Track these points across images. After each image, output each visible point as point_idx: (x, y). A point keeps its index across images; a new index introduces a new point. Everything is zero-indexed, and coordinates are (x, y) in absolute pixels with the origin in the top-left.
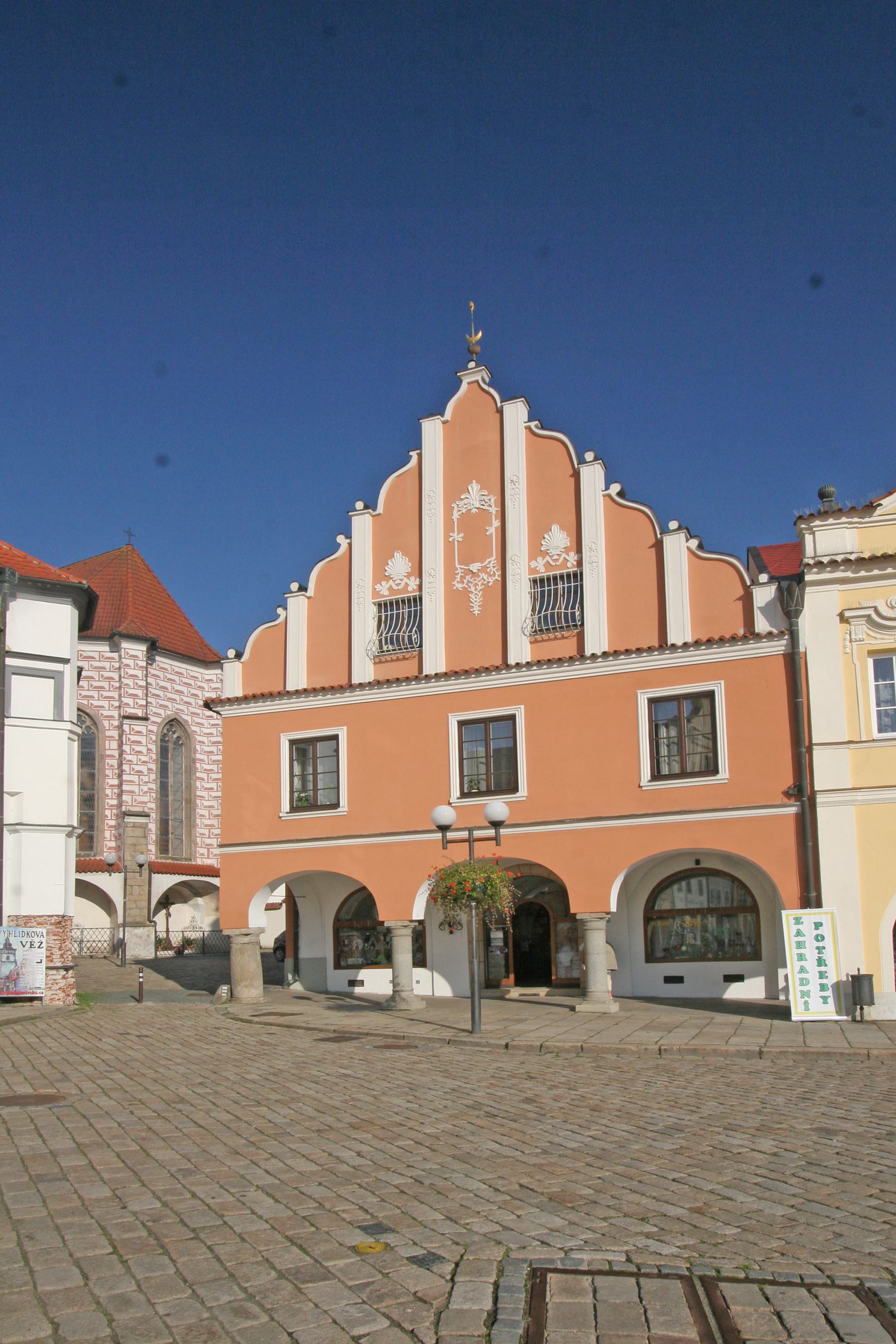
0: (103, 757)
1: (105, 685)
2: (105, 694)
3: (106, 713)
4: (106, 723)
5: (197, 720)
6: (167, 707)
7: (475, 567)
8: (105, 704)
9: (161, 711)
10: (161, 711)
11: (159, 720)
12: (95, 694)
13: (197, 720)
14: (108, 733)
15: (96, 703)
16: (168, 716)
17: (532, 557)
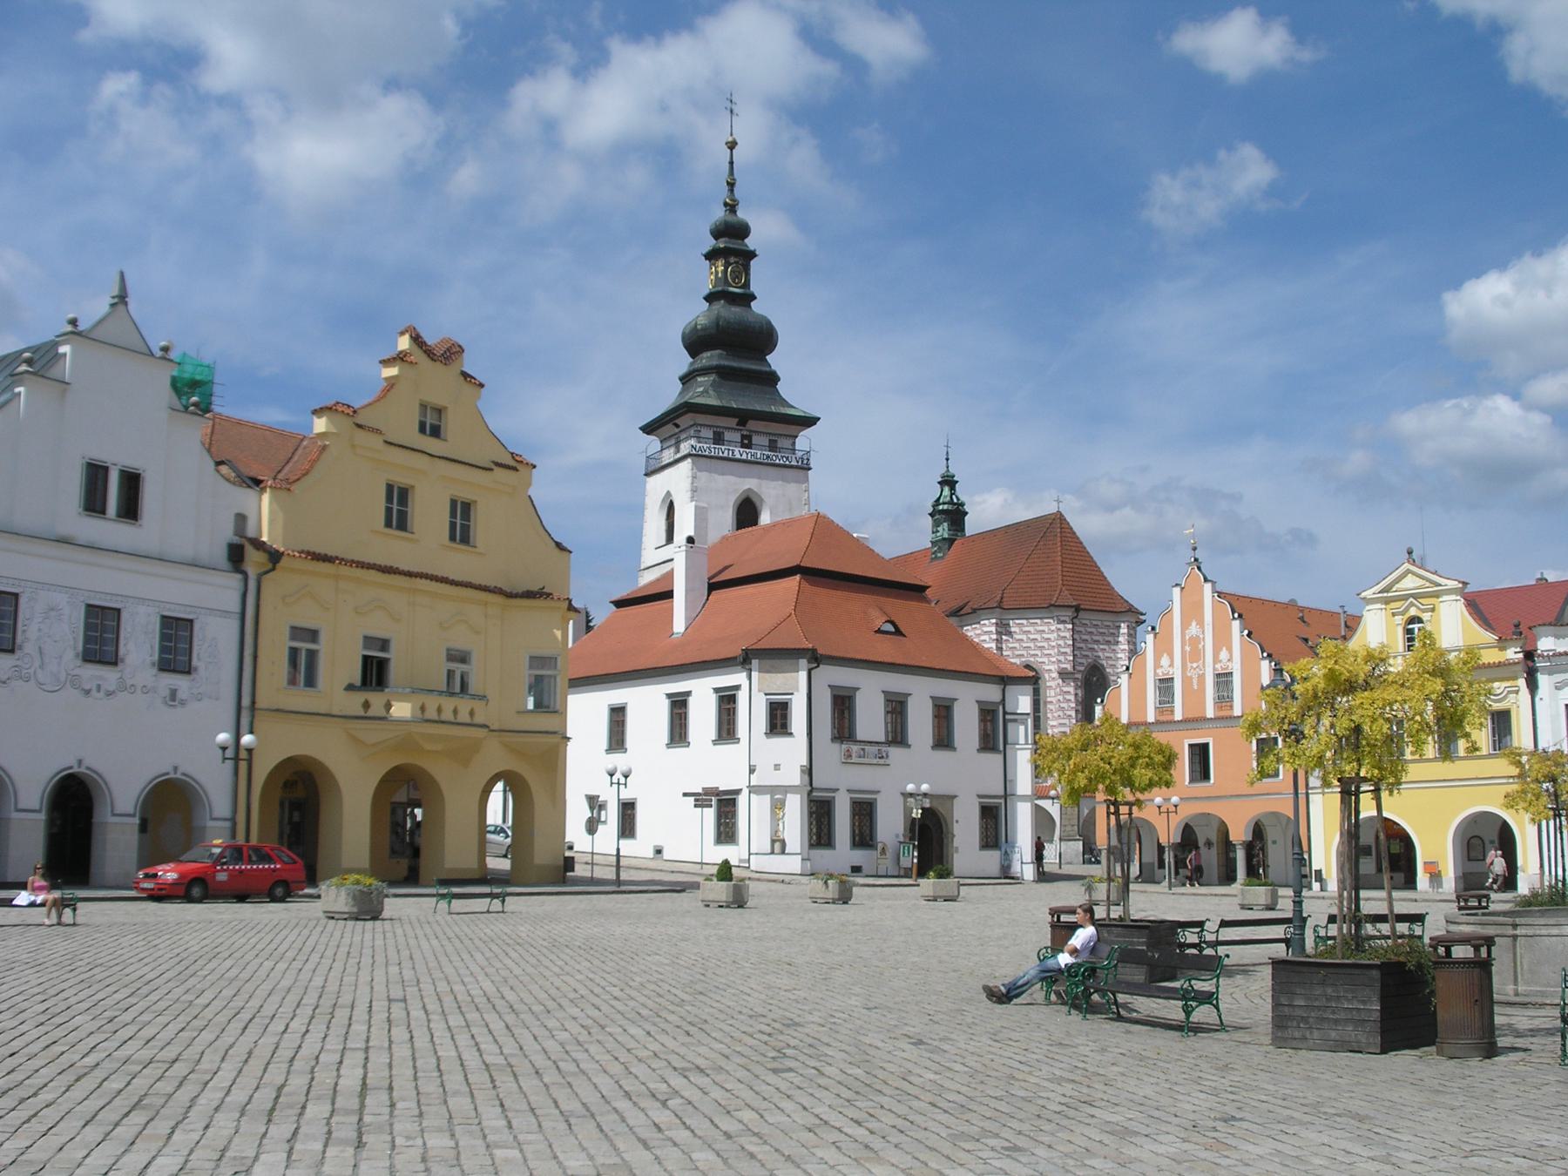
0: (1046, 703)
1: (1045, 644)
2: (1046, 652)
3: (1047, 668)
4: (1046, 676)
5: (1110, 662)
6: (1087, 656)
7: (1195, 665)
8: (1045, 660)
9: (1083, 661)
10: (1083, 661)
11: (1082, 668)
12: (1038, 653)
13: (1110, 662)
14: (1048, 684)
15: (1040, 660)
16: (1089, 664)
17: (1215, 663)
